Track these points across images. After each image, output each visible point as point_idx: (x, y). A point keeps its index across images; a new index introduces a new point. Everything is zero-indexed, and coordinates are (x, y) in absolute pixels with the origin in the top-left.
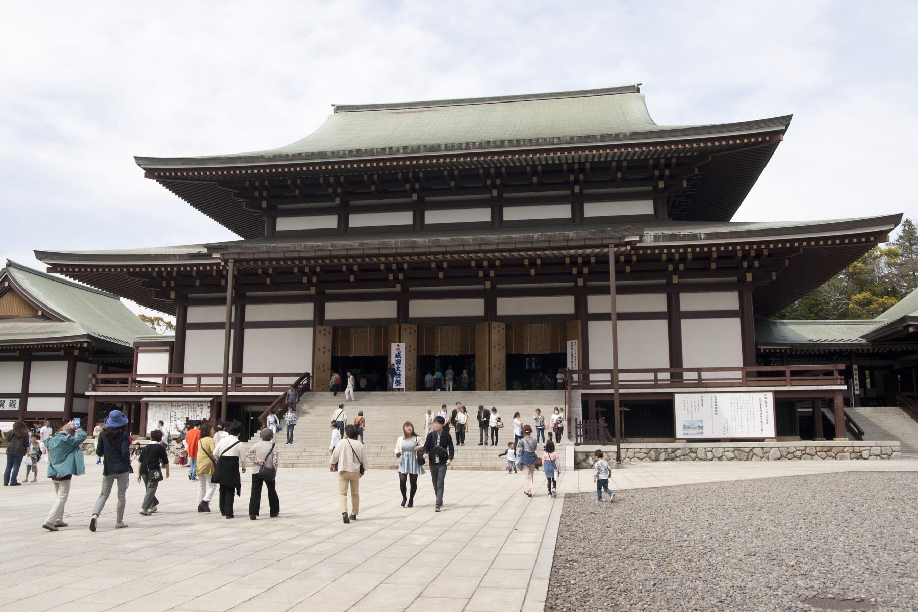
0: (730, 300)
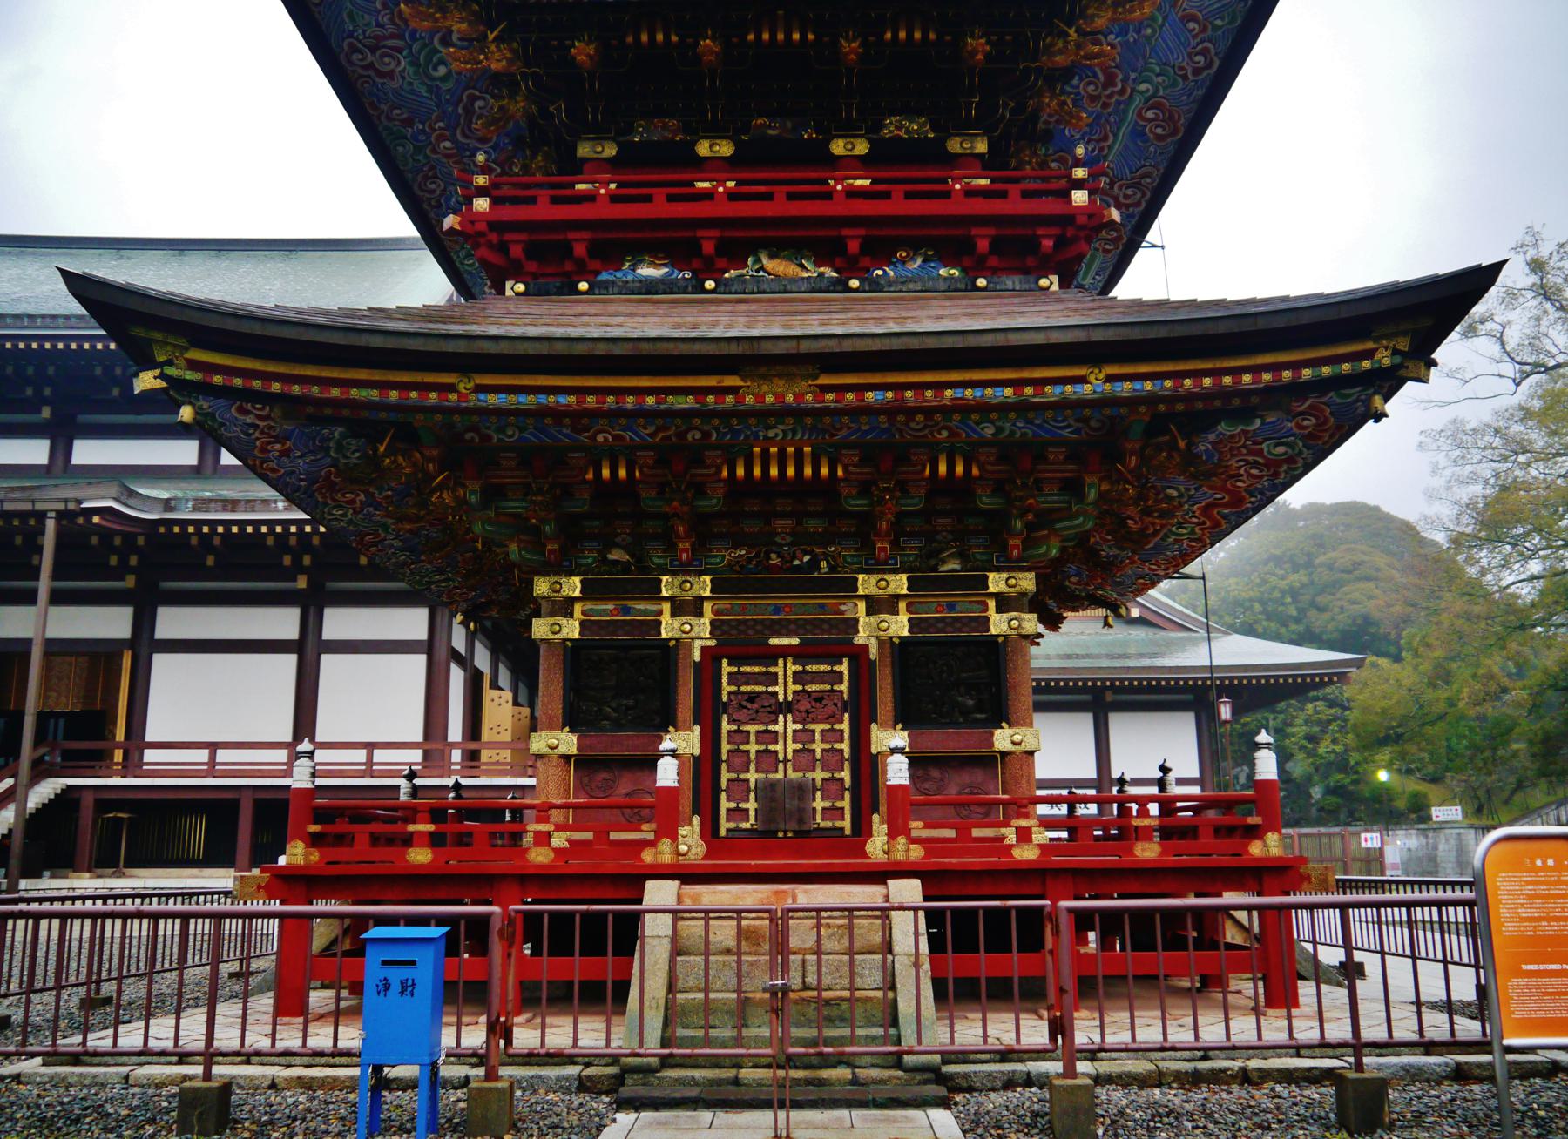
0: (412, 622)
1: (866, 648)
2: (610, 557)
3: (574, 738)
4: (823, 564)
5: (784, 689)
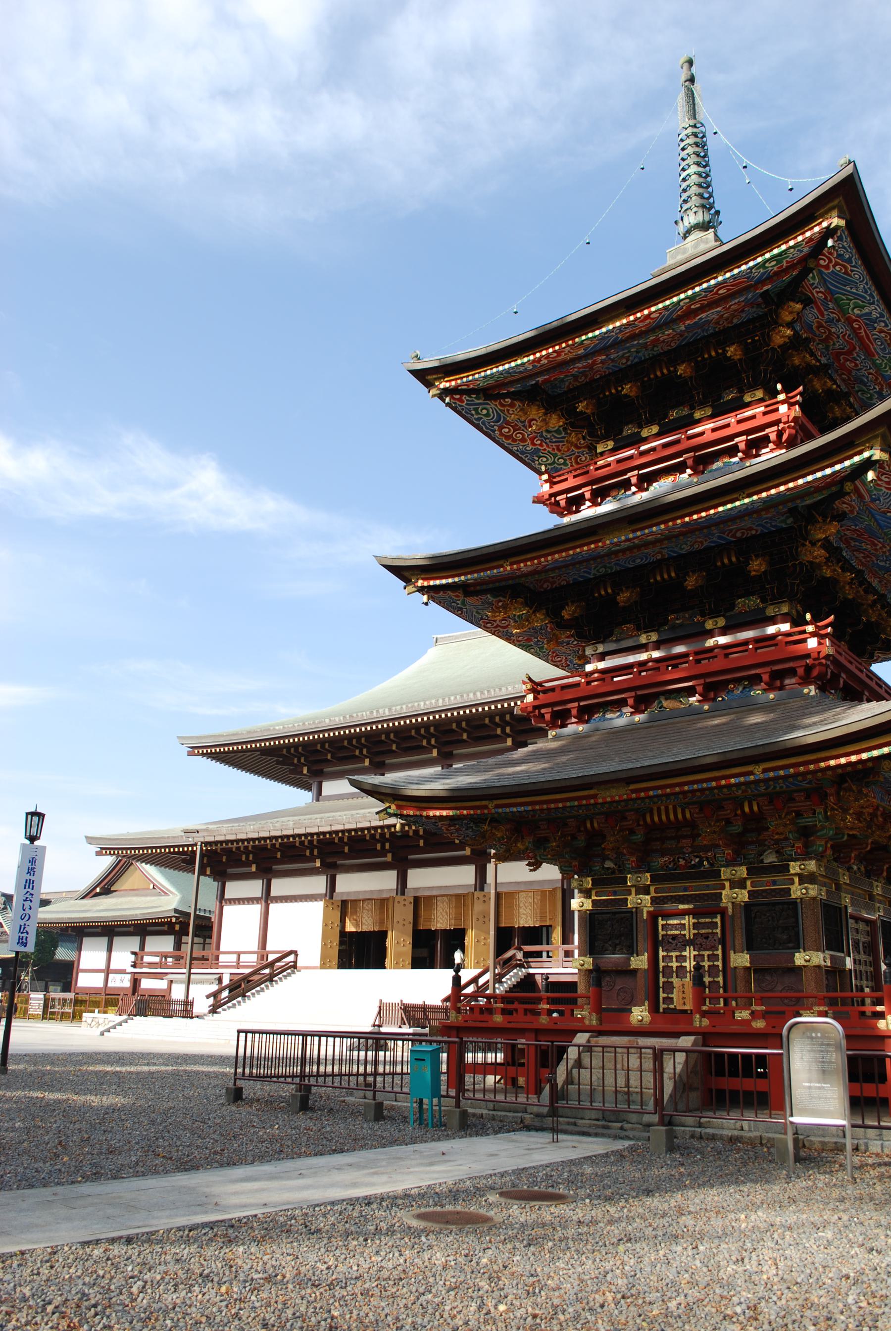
1: (726, 908)
3: (591, 960)
4: (705, 863)
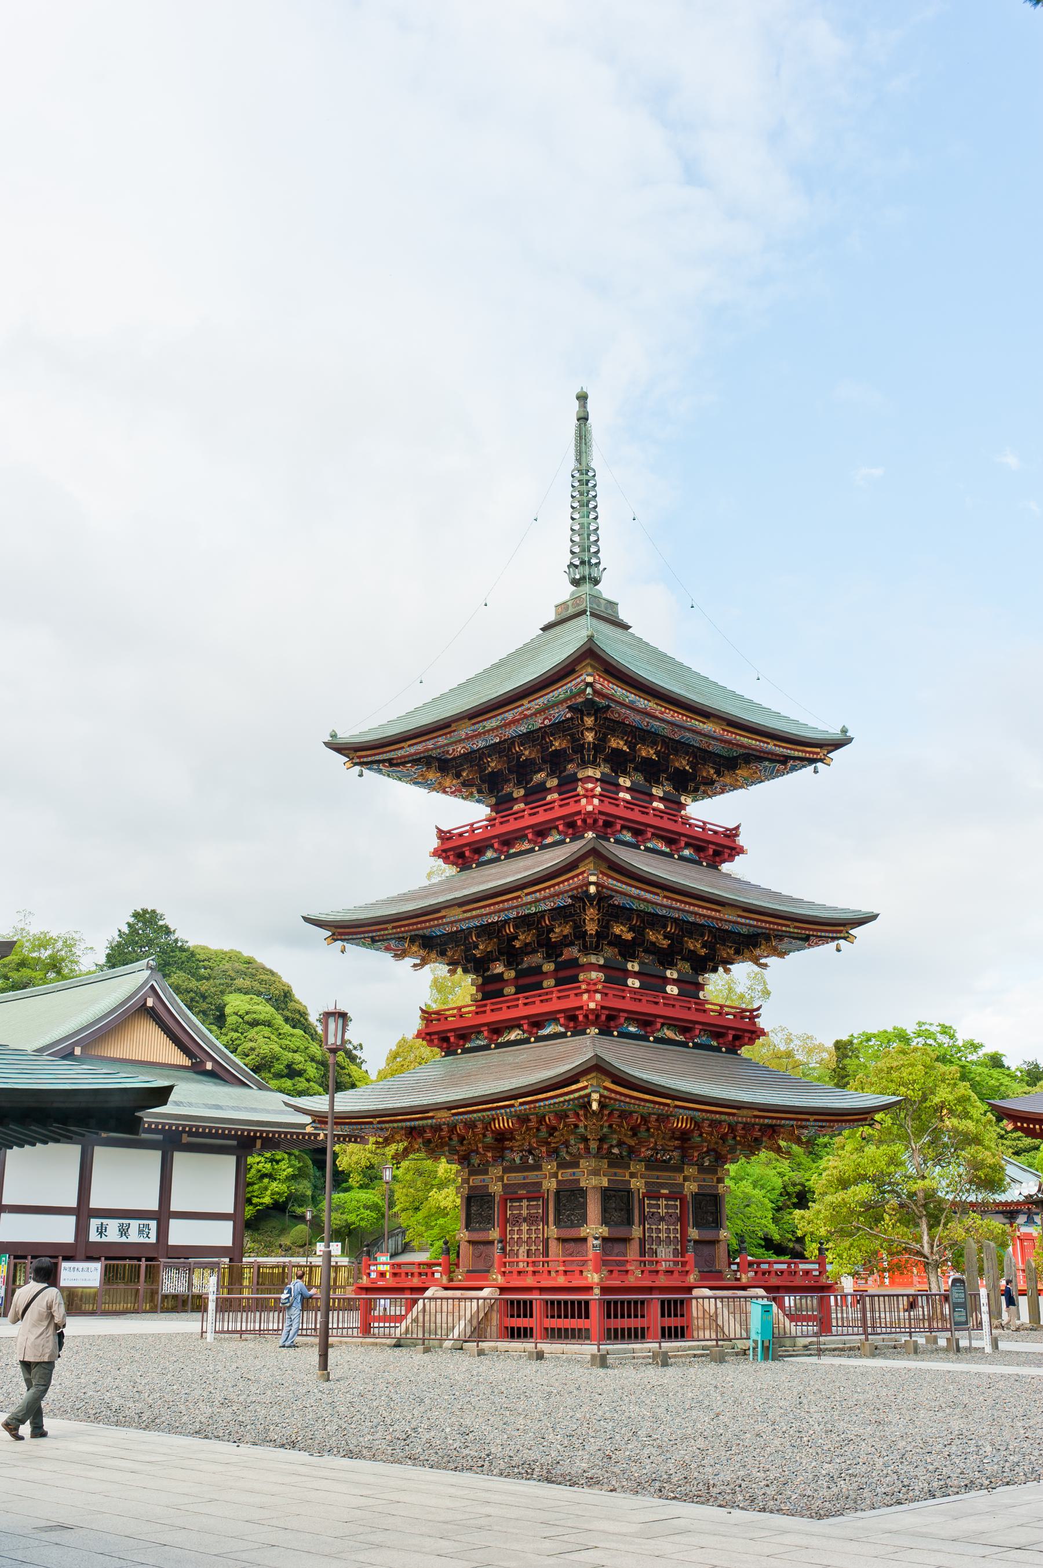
2: (613, 1151)
5: (662, 1211)
